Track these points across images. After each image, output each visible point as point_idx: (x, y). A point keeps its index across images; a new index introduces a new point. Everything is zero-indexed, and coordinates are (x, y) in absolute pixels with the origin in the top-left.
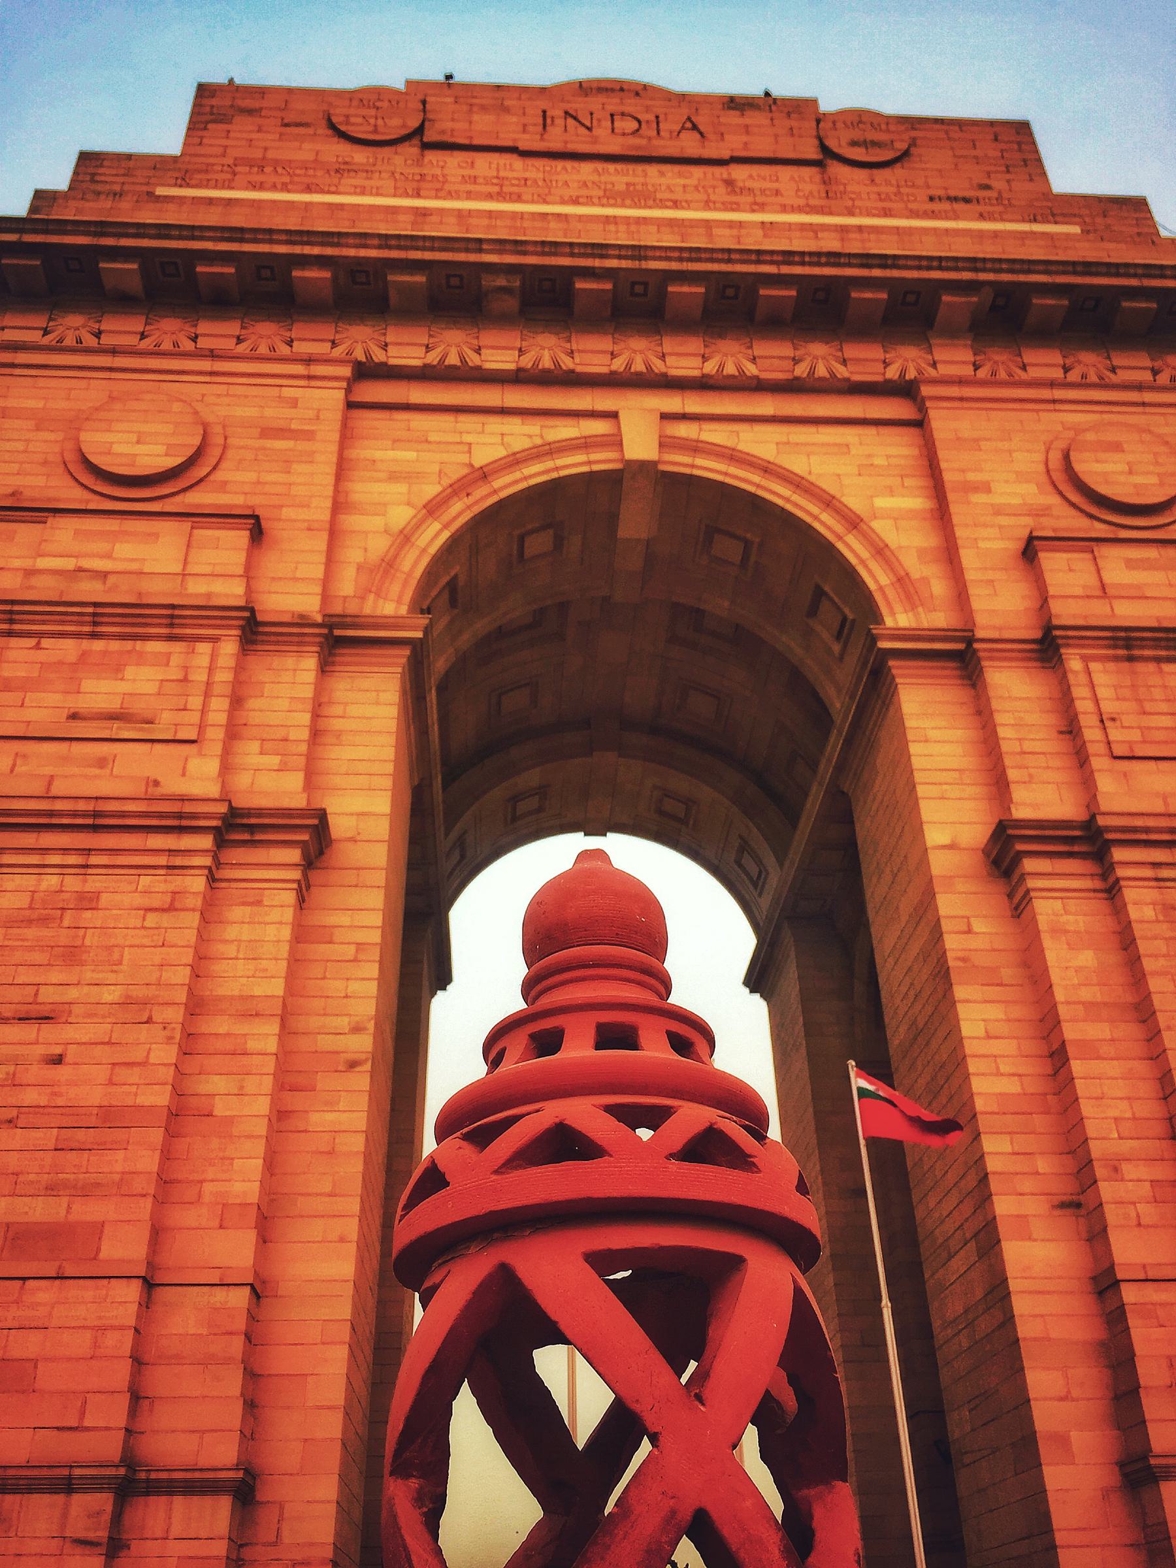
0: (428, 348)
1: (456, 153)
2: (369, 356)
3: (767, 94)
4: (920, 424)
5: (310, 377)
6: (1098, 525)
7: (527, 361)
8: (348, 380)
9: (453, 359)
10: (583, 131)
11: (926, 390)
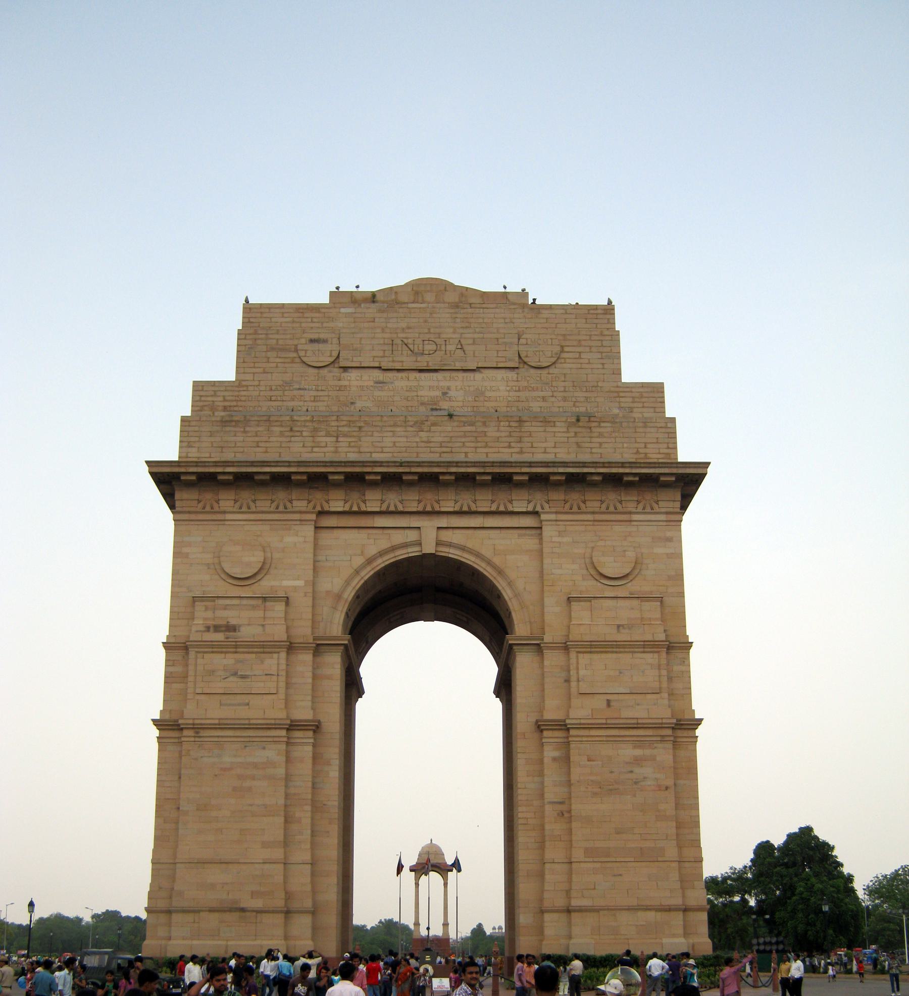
0: (346, 502)
1: (353, 370)
2: (322, 507)
3: (505, 287)
4: (541, 528)
5: (300, 520)
6: (599, 584)
7: (384, 508)
8: (315, 522)
9: (355, 508)
10: (409, 352)
11: (543, 517)
